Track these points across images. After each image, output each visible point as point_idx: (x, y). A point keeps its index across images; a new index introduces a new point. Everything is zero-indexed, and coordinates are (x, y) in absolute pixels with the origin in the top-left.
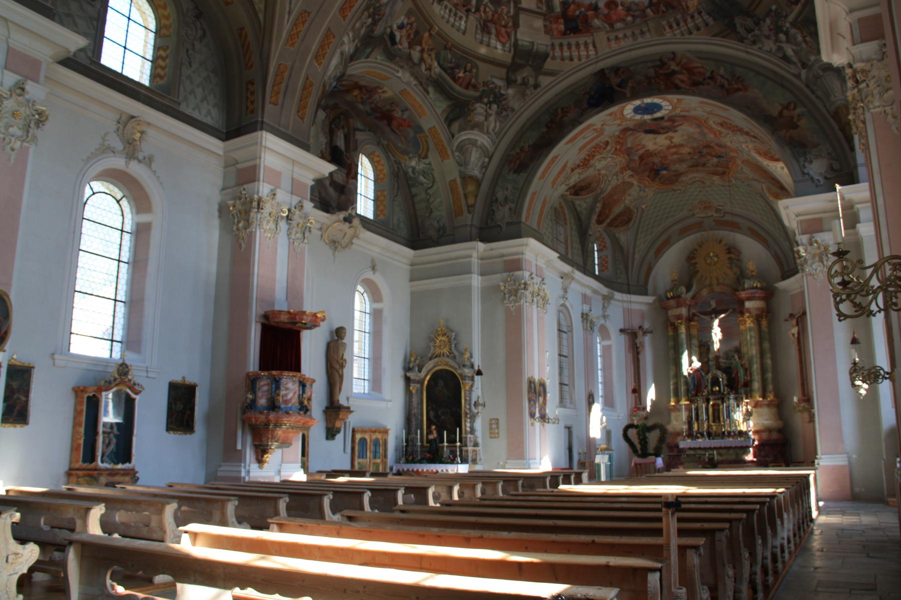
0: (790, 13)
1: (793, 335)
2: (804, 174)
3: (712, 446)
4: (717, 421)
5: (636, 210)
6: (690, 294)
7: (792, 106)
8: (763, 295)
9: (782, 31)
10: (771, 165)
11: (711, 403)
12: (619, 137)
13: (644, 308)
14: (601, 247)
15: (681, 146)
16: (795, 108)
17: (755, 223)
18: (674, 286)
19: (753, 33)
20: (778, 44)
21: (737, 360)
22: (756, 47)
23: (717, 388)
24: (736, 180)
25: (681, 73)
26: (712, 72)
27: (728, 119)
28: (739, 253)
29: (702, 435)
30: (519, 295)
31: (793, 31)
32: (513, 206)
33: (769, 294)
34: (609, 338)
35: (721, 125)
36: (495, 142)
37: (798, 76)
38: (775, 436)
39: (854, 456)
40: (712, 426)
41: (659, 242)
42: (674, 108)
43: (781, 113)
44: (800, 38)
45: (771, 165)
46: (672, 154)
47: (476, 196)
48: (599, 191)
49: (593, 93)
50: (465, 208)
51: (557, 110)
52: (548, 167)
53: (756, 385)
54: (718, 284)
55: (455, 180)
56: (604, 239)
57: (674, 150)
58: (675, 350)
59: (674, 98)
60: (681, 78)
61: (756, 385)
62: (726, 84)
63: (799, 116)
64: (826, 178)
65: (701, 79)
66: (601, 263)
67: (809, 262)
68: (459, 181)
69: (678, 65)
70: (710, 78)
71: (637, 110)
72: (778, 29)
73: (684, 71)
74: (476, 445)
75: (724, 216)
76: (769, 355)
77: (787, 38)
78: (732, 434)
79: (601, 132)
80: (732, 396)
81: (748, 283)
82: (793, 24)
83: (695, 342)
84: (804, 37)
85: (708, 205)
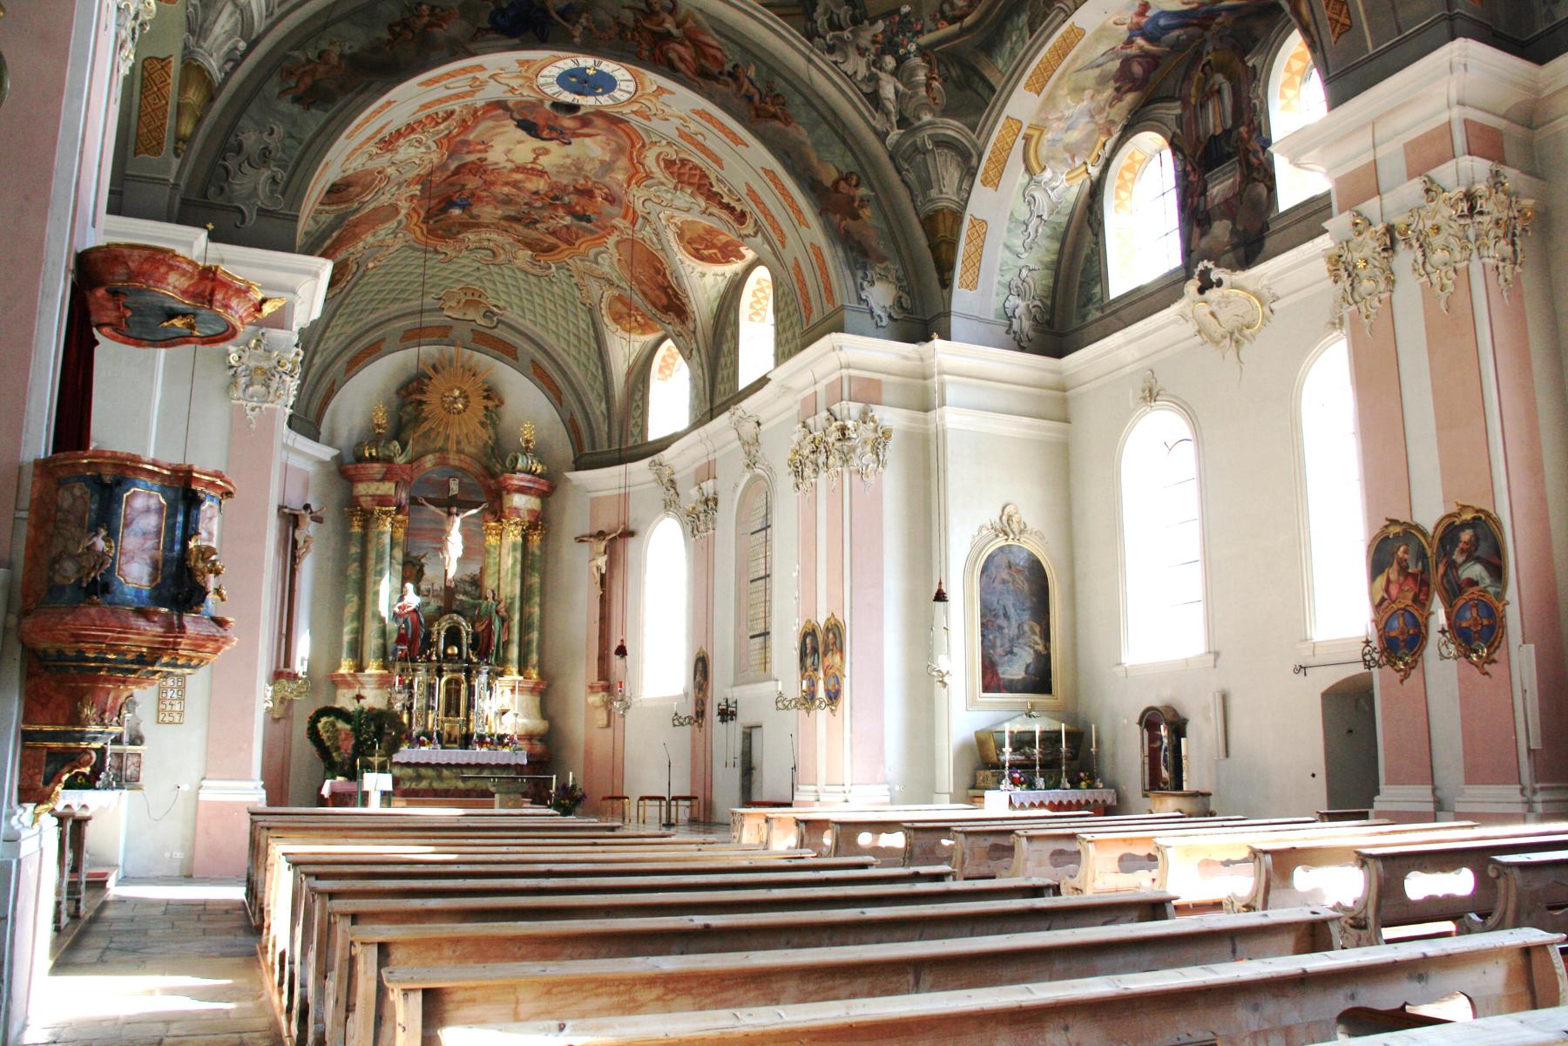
0: (930, 31)
1: (598, 568)
2: (860, 299)
3: (453, 762)
4: (453, 712)
5: (355, 267)
7: (854, 182)
9: (895, 54)
10: (687, 262)
12: (476, 111)
13: (310, 468)
15: (542, 173)
16: (857, 186)
17: (546, 352)
18: (373, 436)
19: (838, 33)
20: (873, 69)
22: (830, 58)
24: (557, 268)
25: (682, 44)
26: (736, 66)
27: (718, 161)
28: (502, 403)
30: (274, 384)
31: (917, 61)
32: (281, 175)
33: (549, 488)
35: (669, 164)
36: (272, 14)
37: (882, 136)
39: (897, 788)
41: (366, 341)
42: (630, 102)
43: (836, 183)
44: (921, 77)
45: (687, 262)
46: (507, 184)
47: (199, 121)
48: (356, 205)
49: (505, 5)
50: (168, 145)
51: (420, 4)
52: (367, 120)
53: (514, 652)
54: (459, 452)
55: (165, 62)
57: (519, 176)
59: (653, 80)
60: (679, 51)
61: (514, 652)
62: (757, 98)
63: (862, 200)
64: (890, 317)
65: (716, 72)
67: (859, 451)
68: (175, 66)
69: (678, 26)
70: (730, 74)
71: (564, 80)
72: (889, 45)
73: (687, 43)
74: (137, 739)
76: (537, 599)
77: (897, 68)
78: (488, 740)
79: (477, 86)
80: (485, 669)
82: (922, 51)
83: (399, 554)
84: (930, 79)
85: (476, 298)
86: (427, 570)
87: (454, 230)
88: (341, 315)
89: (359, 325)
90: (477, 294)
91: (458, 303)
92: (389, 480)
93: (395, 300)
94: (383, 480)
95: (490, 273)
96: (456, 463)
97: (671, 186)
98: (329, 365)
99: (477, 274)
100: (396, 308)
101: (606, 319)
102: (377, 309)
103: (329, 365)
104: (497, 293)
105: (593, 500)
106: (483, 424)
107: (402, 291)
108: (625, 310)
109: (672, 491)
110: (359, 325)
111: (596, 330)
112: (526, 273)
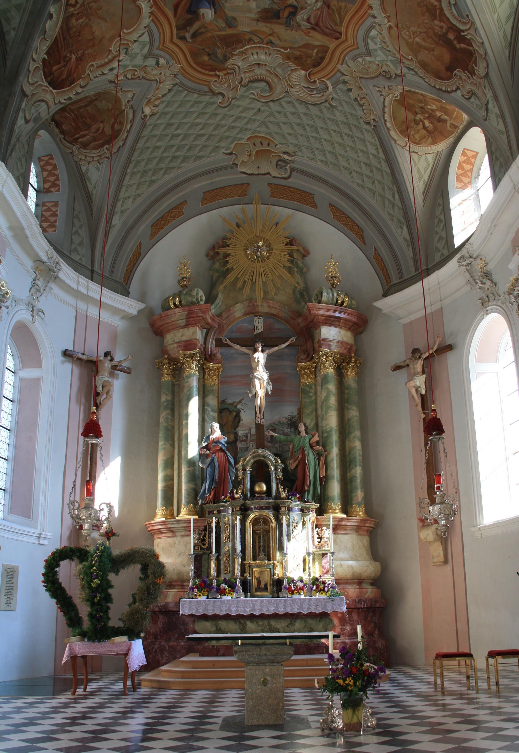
3: (257, 613)
4: (262, 556)
5: (131, 116)
6: (213, 310)
8: (354, 319)
11: (252, 516)
14: (47, 186)
21: (303, 433)
23: (264, 487)
24: (334, 85)
29: (232, 587)
34: (38, 364)
38: (370, 592)
40: (250, 566)
56: (55, 168)
58: (173, 411)
66: (43, 215)
75: (289, 177)
81: (328, 294)
85: (265, 148)
86: (242, 415)
87: (220, 52)
88: (133, 174)
89: (154, 187)
90: (265, 143)
91: (250, 155)
92: (194, 324)
93: (186, 158)
94: (187, 326)
95: (271, 114)
96: (266, 310)
98: (132, 228)
99: (260, 117)
100: (190, 165)
101: (392, 133)
102: (171, 169)
103: (132, 228)
104: (284, 137)
105: (405, 326)
106: (290, 270)
107: (192, 147)
108: (410, 116)
109: (488, 283)
110: (154, 187)
111: (385, 152)
112: (305, 103)
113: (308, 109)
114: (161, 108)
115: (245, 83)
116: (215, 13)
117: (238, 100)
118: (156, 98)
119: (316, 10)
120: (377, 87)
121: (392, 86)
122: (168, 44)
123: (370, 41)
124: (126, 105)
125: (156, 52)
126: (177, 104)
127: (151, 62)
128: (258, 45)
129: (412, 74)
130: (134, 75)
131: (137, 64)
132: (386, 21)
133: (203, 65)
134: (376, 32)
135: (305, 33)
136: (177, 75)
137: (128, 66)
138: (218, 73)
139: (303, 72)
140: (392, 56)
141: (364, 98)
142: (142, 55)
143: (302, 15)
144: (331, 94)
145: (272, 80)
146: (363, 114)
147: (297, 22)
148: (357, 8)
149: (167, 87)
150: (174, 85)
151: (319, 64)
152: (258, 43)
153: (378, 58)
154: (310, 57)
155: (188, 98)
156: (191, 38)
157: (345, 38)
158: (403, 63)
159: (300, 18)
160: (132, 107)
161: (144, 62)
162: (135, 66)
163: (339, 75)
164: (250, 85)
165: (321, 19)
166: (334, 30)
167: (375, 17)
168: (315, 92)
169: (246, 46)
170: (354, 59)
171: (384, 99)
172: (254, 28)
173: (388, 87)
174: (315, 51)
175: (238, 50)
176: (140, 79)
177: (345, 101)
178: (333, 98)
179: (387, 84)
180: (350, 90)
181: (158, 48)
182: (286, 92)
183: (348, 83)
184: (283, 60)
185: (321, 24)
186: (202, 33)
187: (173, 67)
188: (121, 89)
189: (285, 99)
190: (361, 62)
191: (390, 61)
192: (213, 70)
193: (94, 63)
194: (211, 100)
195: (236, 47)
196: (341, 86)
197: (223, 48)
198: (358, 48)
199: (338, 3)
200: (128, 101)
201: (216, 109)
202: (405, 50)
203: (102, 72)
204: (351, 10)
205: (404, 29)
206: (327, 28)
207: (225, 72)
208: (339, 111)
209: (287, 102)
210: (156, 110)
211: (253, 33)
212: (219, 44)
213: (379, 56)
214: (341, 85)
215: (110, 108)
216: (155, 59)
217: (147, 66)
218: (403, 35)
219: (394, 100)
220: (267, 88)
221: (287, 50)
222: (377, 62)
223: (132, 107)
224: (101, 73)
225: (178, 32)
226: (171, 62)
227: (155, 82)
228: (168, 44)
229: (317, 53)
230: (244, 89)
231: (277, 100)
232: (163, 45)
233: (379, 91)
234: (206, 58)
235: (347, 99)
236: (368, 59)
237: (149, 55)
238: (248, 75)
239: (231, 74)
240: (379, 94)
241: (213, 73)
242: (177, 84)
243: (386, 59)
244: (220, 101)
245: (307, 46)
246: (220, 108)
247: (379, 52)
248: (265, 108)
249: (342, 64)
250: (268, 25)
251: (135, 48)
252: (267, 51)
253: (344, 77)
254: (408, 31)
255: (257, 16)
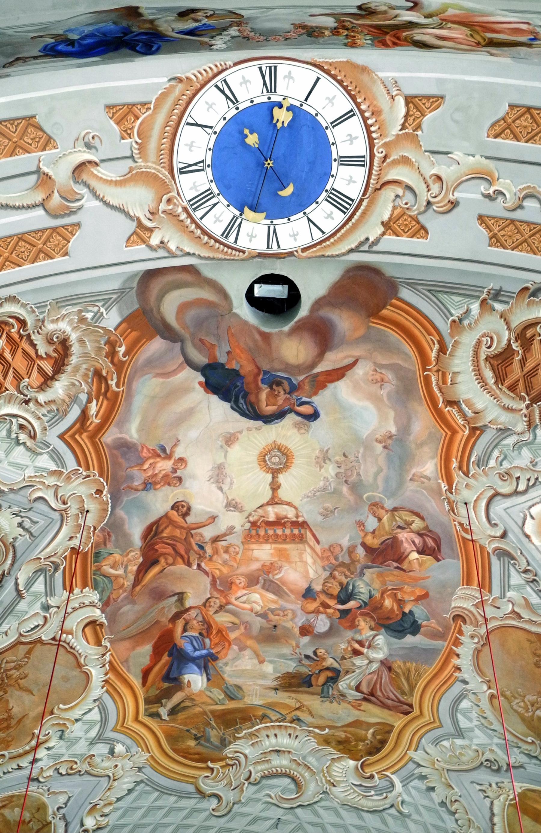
24: (405, 782)
87: (214, 734)
97: (521, 426)
113: (361, 818)
114: (112, 819)
115: (256, 780)
116: (208, 680)
117: (245, 805)
118: (106, 802)
119: (370, 674)
120: (478, 784)
121: (503, 782)
122: (130, 723)
123: (460, 716)
124: (54, 814)
125: (109, 734)
126: (140, 812)
127: (102, 749)
128: (278, 724)
129: (535, 764)
130: (72, 769)
131: (78, 753)
132: (485, 687)
133: (186, 754)
134: (470, 703)
135: (352, 706)
136: (143, 767)
137: (63, 755)
138: (210, 764)
139: (352, 763)
140: (499, 738)
141: (456, 801)
142: (86, 739)
143: (348, 682)
144: (400, 795)
145: (301, 775)
146: (456, 826)
147: (339, 692)
148: (436, 670)
149: (126, 785)
150: (137, 783)
151: (378, 750)
152: (277, 721)
153: (475, 741)
154: (363, 740)
155: (159, 803)
156: (168, 715)
157: (418, 713)
158: (520, 747)
159: (345, 686)
160: (64, 817)
161: (89, 750)
162: (75, 755)
163: (411, 766)
164: (264, 782)
165: (378, 686)
166: (400, 702)
167: (465, 682)
168: (373, 793)
169: (258, 725)
170: (436, 742)
171: (492, 803)
172: (270, 700)
173: (497, 784)
174: (371, 731)
175: (245, 732)
176: (80, 775)
177: (425, 807)
178: (403, 802)
179: (494, 779)
180: (432, 789)
181: (114, 730)
182: (324, 792)
183: (427, 778)
184: (318, 744)
185: (379, 693)
186: (188, 707)
187: (137, 756)
188: (49, 790)
189: (323, 803)
190: (448, 746)
191: (497, 744)
192: (204, 760)
193: (5, 753)
194: (199, 806)
195: (241, 728)
196: (416, 783)
197: (220, 729)
198: (441, 726)
199: (405, 663)
200: (59, 809)
201: (206, 819)
202: (520, 728)
203: (18, 765)
204: (425, 673)
205: (515, 698)
206: (388, 698)
207: (223, 763)
208: (415, 822)
209: (325, 808)
210: (104, 821)
211: (270, 706)
212: (213, 723)
213: (477, 737)
214: (416, 781)
215: (27, 820)
216: (109, 746)
217: (94, 756)
218: (515, 707)
219: (509, 804)
220: (292, 786)
221: (325, 730)
222: (474, 747)
223: (64, 817)
224: (17, 767)
225: (147, 707)
226: (135, 749)
227: (107, 778)
228: (130, 723)
229: (374, 734)
230: (253, 788)
231: (309, 805)
232: (122, 726)
233: (480, 790)
234: (192, 743)
235: (426, 803)
236: (459, 742)
237: (99, 739)
238: (259, 767)
239: (232, 765)
240: (481, 795)
241: (203, 765)
242: (142, 781)
243: (489, 742)
244: (214, 806)
245: (357, 724)
246: (214, 818)
247: (477, 732)
248: (289, 817)
249: (416, 750)
250: (293, 695)
251: (77, 730)
252: (290, 731)
253: (421, 769)
254: (523, 701)
255: (276, 683)
